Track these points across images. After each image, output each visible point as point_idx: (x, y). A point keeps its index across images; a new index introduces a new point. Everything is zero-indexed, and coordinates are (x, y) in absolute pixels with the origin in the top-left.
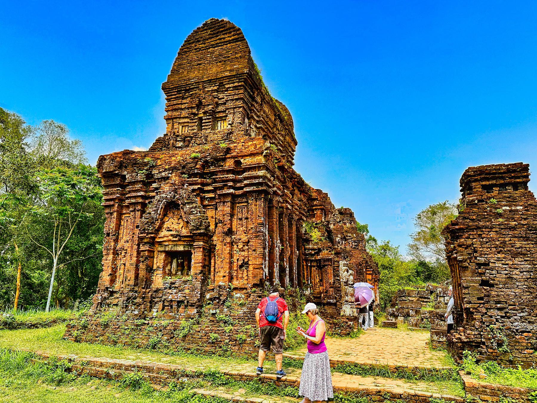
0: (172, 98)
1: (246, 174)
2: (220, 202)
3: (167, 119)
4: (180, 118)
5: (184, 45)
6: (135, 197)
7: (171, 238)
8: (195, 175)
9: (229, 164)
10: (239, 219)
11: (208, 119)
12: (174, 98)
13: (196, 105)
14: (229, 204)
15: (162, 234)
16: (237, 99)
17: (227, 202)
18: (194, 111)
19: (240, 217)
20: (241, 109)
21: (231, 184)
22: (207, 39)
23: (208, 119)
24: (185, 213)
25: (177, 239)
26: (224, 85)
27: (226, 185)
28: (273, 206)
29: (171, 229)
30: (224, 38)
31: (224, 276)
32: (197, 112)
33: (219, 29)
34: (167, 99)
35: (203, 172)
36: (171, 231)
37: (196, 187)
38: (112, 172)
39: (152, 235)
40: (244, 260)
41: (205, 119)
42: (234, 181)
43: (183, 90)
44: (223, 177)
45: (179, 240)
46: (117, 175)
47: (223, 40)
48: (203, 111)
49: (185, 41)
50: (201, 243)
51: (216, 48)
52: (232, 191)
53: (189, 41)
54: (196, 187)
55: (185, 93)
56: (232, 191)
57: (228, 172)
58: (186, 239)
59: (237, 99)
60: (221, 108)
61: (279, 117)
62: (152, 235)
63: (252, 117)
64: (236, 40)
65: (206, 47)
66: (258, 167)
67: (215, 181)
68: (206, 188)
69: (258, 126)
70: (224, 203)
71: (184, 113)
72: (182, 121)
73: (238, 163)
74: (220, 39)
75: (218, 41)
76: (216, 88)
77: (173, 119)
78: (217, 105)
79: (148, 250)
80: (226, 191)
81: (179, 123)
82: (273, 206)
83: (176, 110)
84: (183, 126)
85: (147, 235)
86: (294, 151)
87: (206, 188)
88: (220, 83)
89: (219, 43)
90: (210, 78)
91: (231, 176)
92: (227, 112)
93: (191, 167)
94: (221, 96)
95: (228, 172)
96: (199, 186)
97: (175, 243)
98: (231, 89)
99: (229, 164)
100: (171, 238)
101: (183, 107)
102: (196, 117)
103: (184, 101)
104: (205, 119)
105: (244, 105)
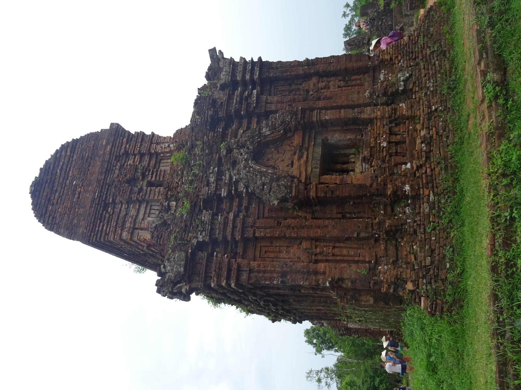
0: (106, 230)
2: (265, 106)
6: (234, 227)
7: (302, 161)
17: (267, 99)
25: (305, 153)
29: (290, 162)
30: (64, 163)
36: (292, 162)
38: (187, 257)
41: (152, 177)
43: (103, 212)
44: (236, 100)
46: (193, 253)
47: (64, 167)
53: (41, 216)
55: (107, 212)
57: (230, 97)
58: (307, 140)
71: (133, 212)
72: (141, 216)
81: (143, 219)
83: (124, 222)
88: (115, 160)
89: (66, 170)
90: (104, 171)
98: (128, 146)
100: (302, 161)
104: (152, 177)
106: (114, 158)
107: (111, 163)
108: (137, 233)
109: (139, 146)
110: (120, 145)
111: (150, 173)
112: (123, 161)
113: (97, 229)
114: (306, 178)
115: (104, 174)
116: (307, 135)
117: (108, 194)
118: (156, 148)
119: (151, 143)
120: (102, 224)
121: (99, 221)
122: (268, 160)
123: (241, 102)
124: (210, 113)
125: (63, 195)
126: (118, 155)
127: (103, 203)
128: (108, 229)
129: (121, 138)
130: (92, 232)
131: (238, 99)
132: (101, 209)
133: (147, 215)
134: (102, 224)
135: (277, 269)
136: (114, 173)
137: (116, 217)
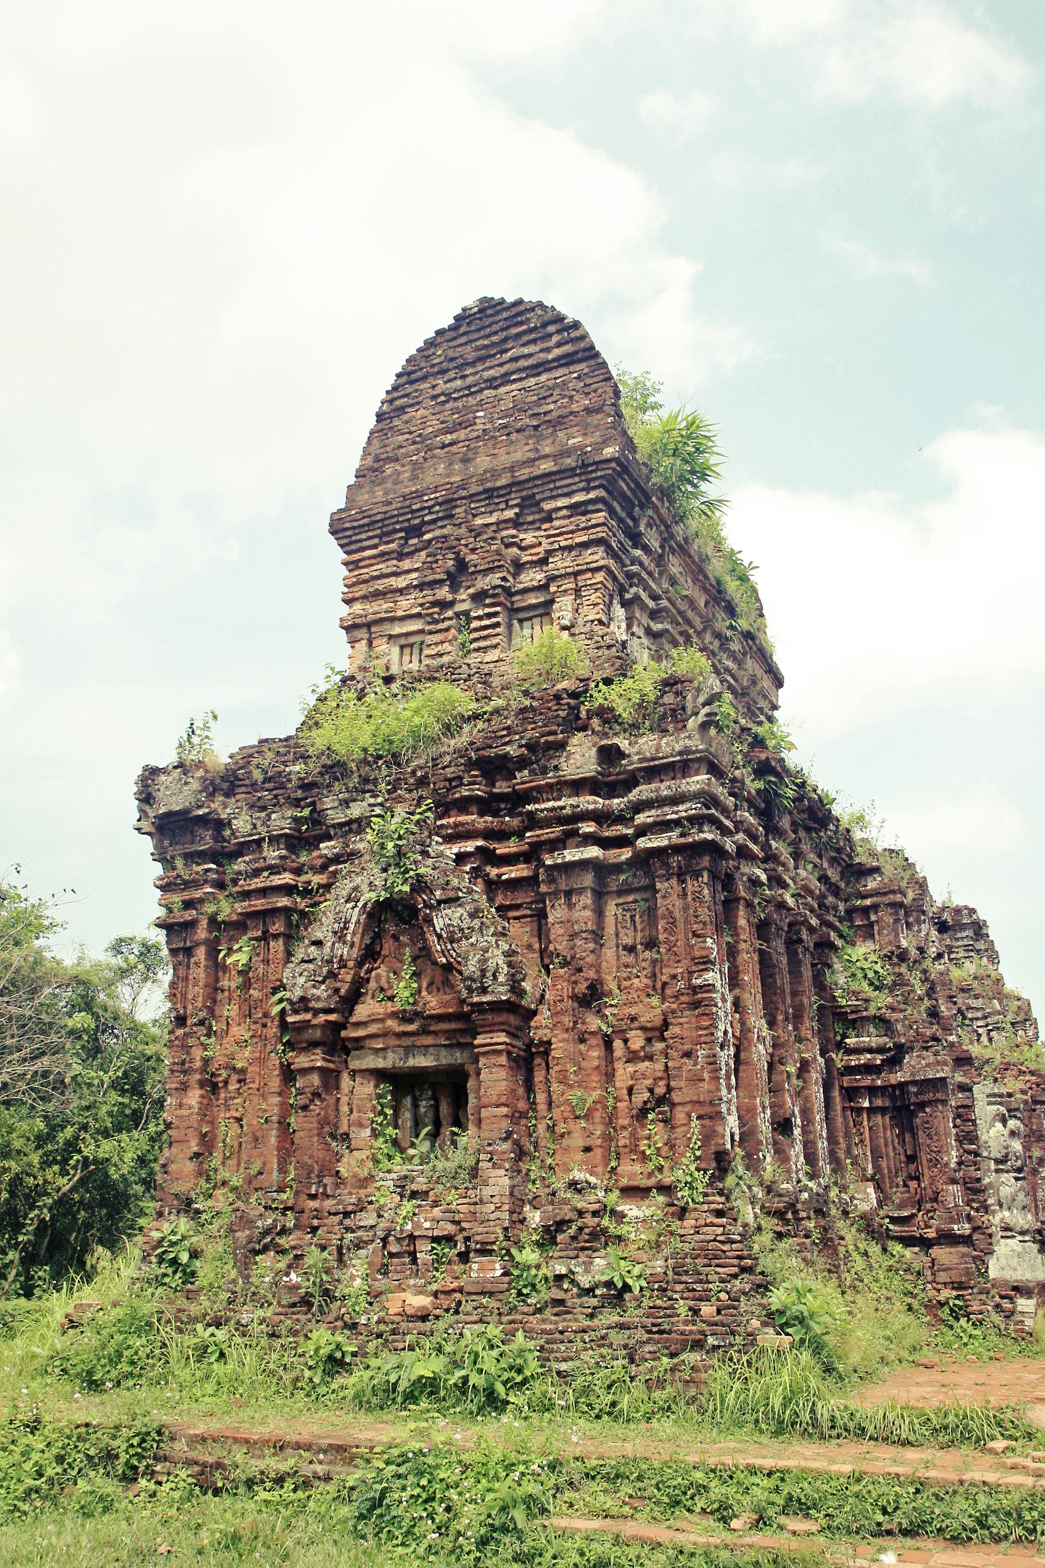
0: (364, 559)
1: (642, 792)
2: (555, 894)
3: (350, 628)
4: (392, 620)
5: (395, 388)
7: (392, 1024)
8: (463, 805)
9: (580, 757)
10: (625, 948)
11: (489, 616)
12: (369, 558)
13: (448, 573)
14: (587, 899)
15: (362, 1011)
16: (585, 545)
17: (581, 891)
18: (444, 593)
19: (629, 941)
20: (600, 577)
21: (588, 828)
22: (473, 364)
23: (489, 616)
24: (439, 937)
25: (412, 1028)
26: (538, 503)
27: (575, 833)
28: (738, 899)
31: (587, 1149)
32: (449, 597)
33: (508, 328)
34: (346, 564)
35: (491, 794)
37: (470, 846)
38: (185, 812)
39: (333, 1017)
40: (651, 1090)
41: (480, 618)
42: (600, 817)
44: (563, 808)
45: (424, 1031)
46: (203, 820)
48: (471, 591)
49: (399, 376)
50: (502, 1038)
51: (503, 390)
52: (594, 852)
53: (409, 374)
54: (470, 846)
56: (594, 852)
57: (578, 786)
59: (585, 545)
60: (533, 577)
61: (717, 595)
62: (333, 1017)
63: (637, 597)
64: (568, 360)
65: (469, 387)
66: (683, 766)
67: (533, 821)
68: (502, 849)
69: (657, 627)
70: (568, 894)
71: (405, 604)
72: (397, 629)
73: (609, 755)
74: (515, 359)
75: (507, 368)
76: (510, 514)
77: (368, 625)
78: (519, 567)
79: (320, 1069)
80: (571, 855)
81: (391, 637)
82: (738, 899)
83: (378, 595)
84: (402, 647)
85: (315, 1015)
86: (775, 707)
87: (502, 849)
88: (523, 499)
89: (513, 373)
90: (489, 485)
91: (589, 802)
92: (553, 589)
93: (450, 780)
94: (528, 538)
95: (578, 786)
96: (480, 843)
97: (407, 1041)
98: (565, 512)
99: (580, 757)
100: (392, 1024)
101: (401, 582)
102: (450, 613)
103: (406, 564)
104: (480, 618)
105: (611, 563)
106: (524, 493)
107: (509, 494)
108: (360, 636)
109: (563, 544)
110: (565, 490)
111: (487, 610)
112: (530, 518)
113: (363, 536)
114: (357, 1039)
115: (481, 489)
116: (453, 1026)
117: (440, 524)
118: (565, 591)
119: (576, 574)
120: (376, 541)
121: (379, 532)
122: (396, 938)
123: (561, 820)
124: (512, 750)
125: (455, 399)
126: (538, 497)
127: (417, 521)
128: (367, 562)
129: (582, 485)
130: (353, 528)
131: (568, 811)
132: (406, 524)
133: (403, 641)
134: (376, 541)
135: (190, 1007)
136: (491, 512)
137: (389, 571)
